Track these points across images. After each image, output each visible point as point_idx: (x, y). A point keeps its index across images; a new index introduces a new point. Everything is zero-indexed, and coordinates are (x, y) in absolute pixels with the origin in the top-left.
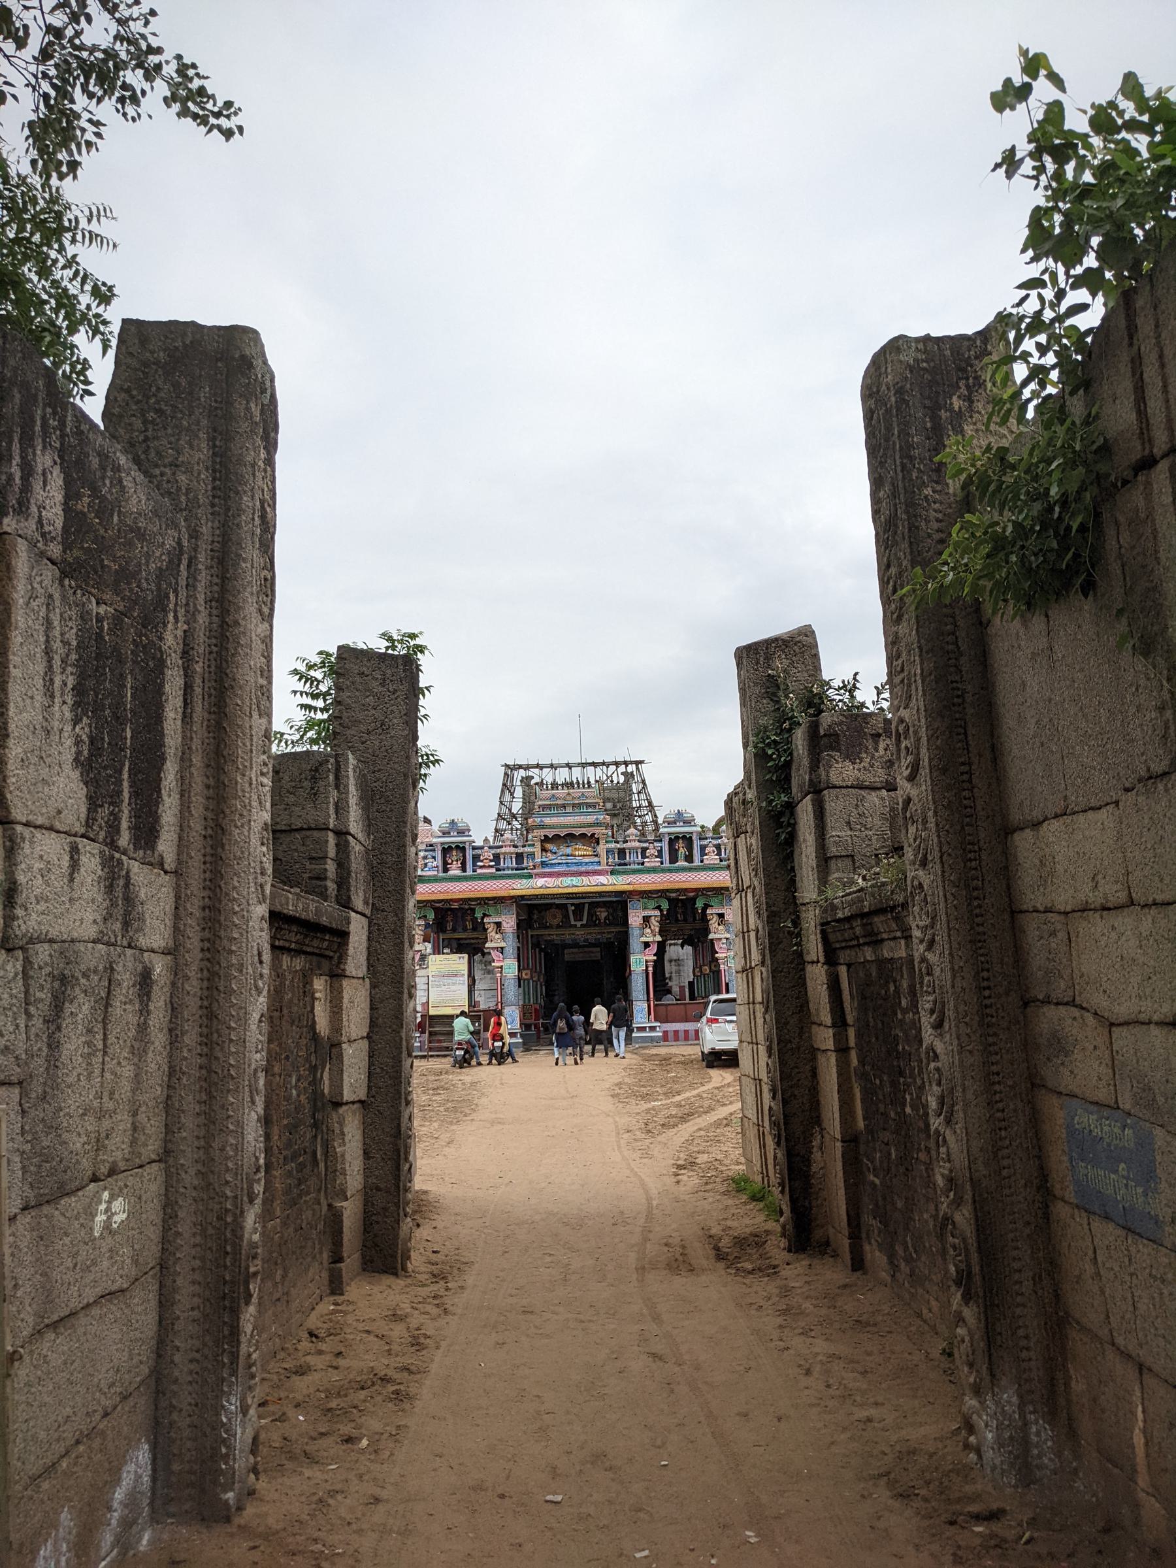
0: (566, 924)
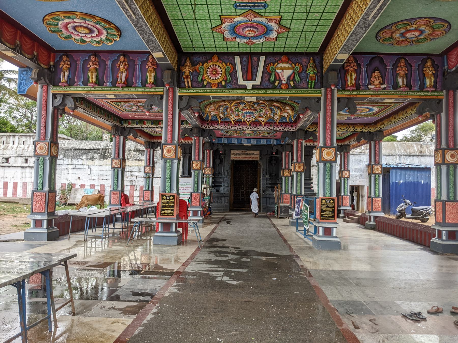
0: (230, 82)
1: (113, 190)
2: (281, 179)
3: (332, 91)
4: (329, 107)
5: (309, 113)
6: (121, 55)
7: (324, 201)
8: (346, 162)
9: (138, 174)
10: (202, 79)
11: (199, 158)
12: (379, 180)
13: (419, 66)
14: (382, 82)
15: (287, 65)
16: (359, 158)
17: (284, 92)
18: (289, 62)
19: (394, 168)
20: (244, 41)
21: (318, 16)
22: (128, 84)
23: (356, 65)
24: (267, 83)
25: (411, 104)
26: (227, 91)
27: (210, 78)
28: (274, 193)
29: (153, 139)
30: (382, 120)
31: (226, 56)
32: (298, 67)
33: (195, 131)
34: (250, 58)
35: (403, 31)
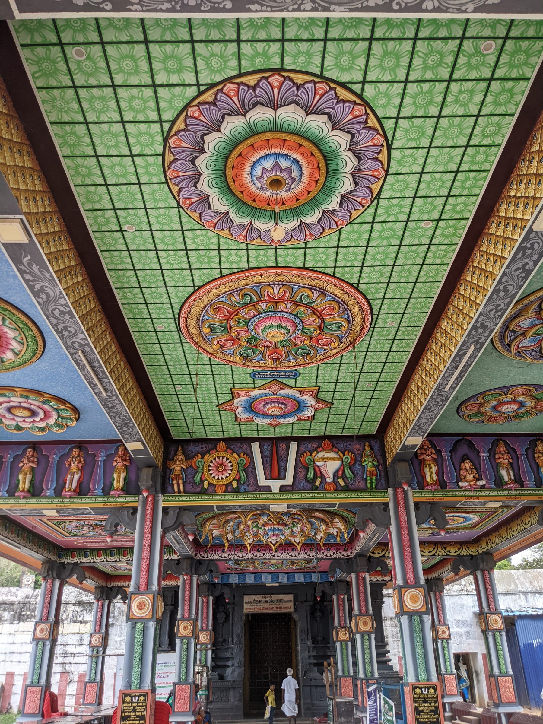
0: (246, 482)
1: (32, 685)
2: (335, 647)
3: (405, 493)
4: (404, 519)
5: (372, 527)
6: (75, 447)
7: (418, 691)
8: (440, 609)
9: (79, 649)
10: (201, 479)
11: (190, 613)
12: (502, 641)
13: (526, 450)
14: (477, 476)
15: (331, 454)
16: (460, 600)
17: (331, 496)
18: (334, 449)
19: (520, 617)
20: (266, 421)
21: (371, 386)
22: (82, 491)
23: (434, 452)
24: (303, 482)
25: (527, 509)
26: (241, 497)
27: (214, 477)
28: (324, 675)
29: (111, 581)
30: (487, 535)
31: (238, 444)
32: (348, 457)
33: (185, 564)
34: (274, 446)
35: (494, 403)
